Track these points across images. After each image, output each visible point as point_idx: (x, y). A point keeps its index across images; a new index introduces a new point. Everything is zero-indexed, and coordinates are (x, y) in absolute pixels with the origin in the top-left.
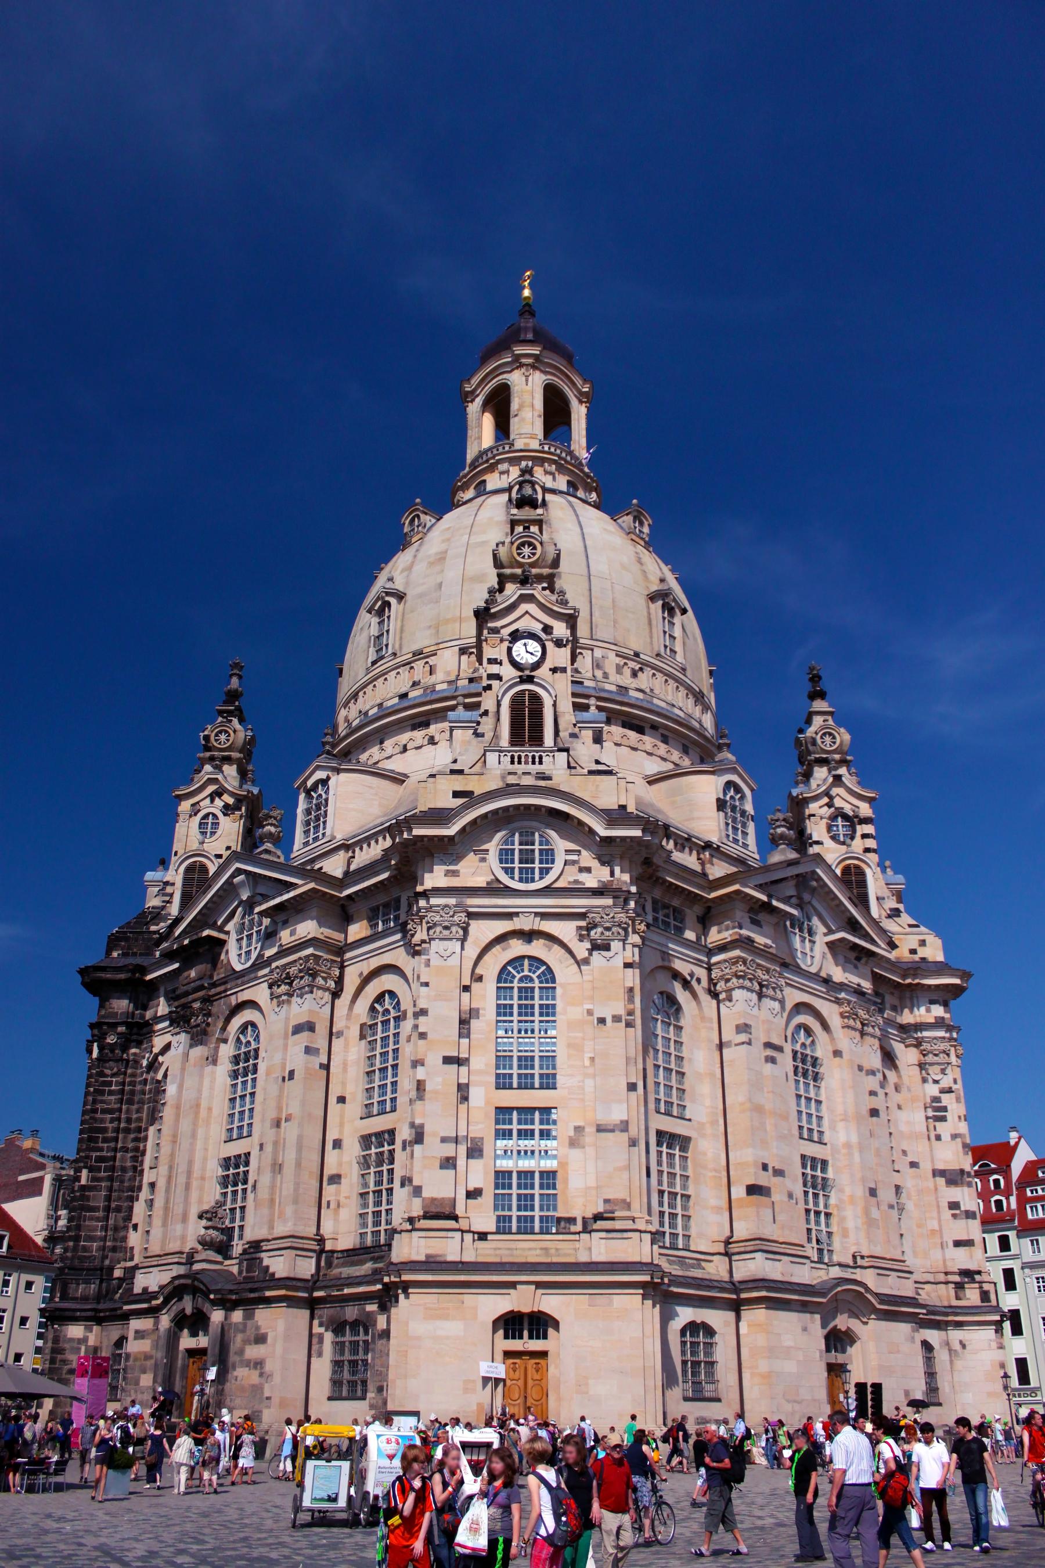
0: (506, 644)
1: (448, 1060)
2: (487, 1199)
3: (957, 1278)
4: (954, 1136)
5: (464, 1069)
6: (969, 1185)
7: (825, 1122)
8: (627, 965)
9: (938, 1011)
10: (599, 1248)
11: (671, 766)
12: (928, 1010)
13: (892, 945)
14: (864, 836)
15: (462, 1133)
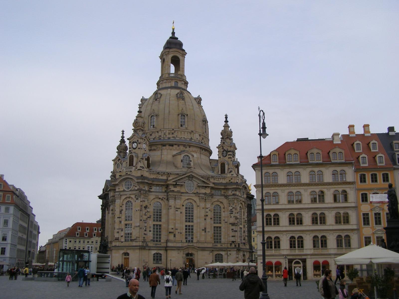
0: (132, 144)
1: (118, 218)
2: (124, 237)
3: (231, 243)
4: (234, 217)
5: (120, 219)
6: (236, 226)
7: (194, 219)
8: (141, 201)
9: (233, 192)
10: (134, 244)
11: (180, 151)
12: (231, 192)
13: (214, 183)
14: (229, 155)
15: (120, 228)
